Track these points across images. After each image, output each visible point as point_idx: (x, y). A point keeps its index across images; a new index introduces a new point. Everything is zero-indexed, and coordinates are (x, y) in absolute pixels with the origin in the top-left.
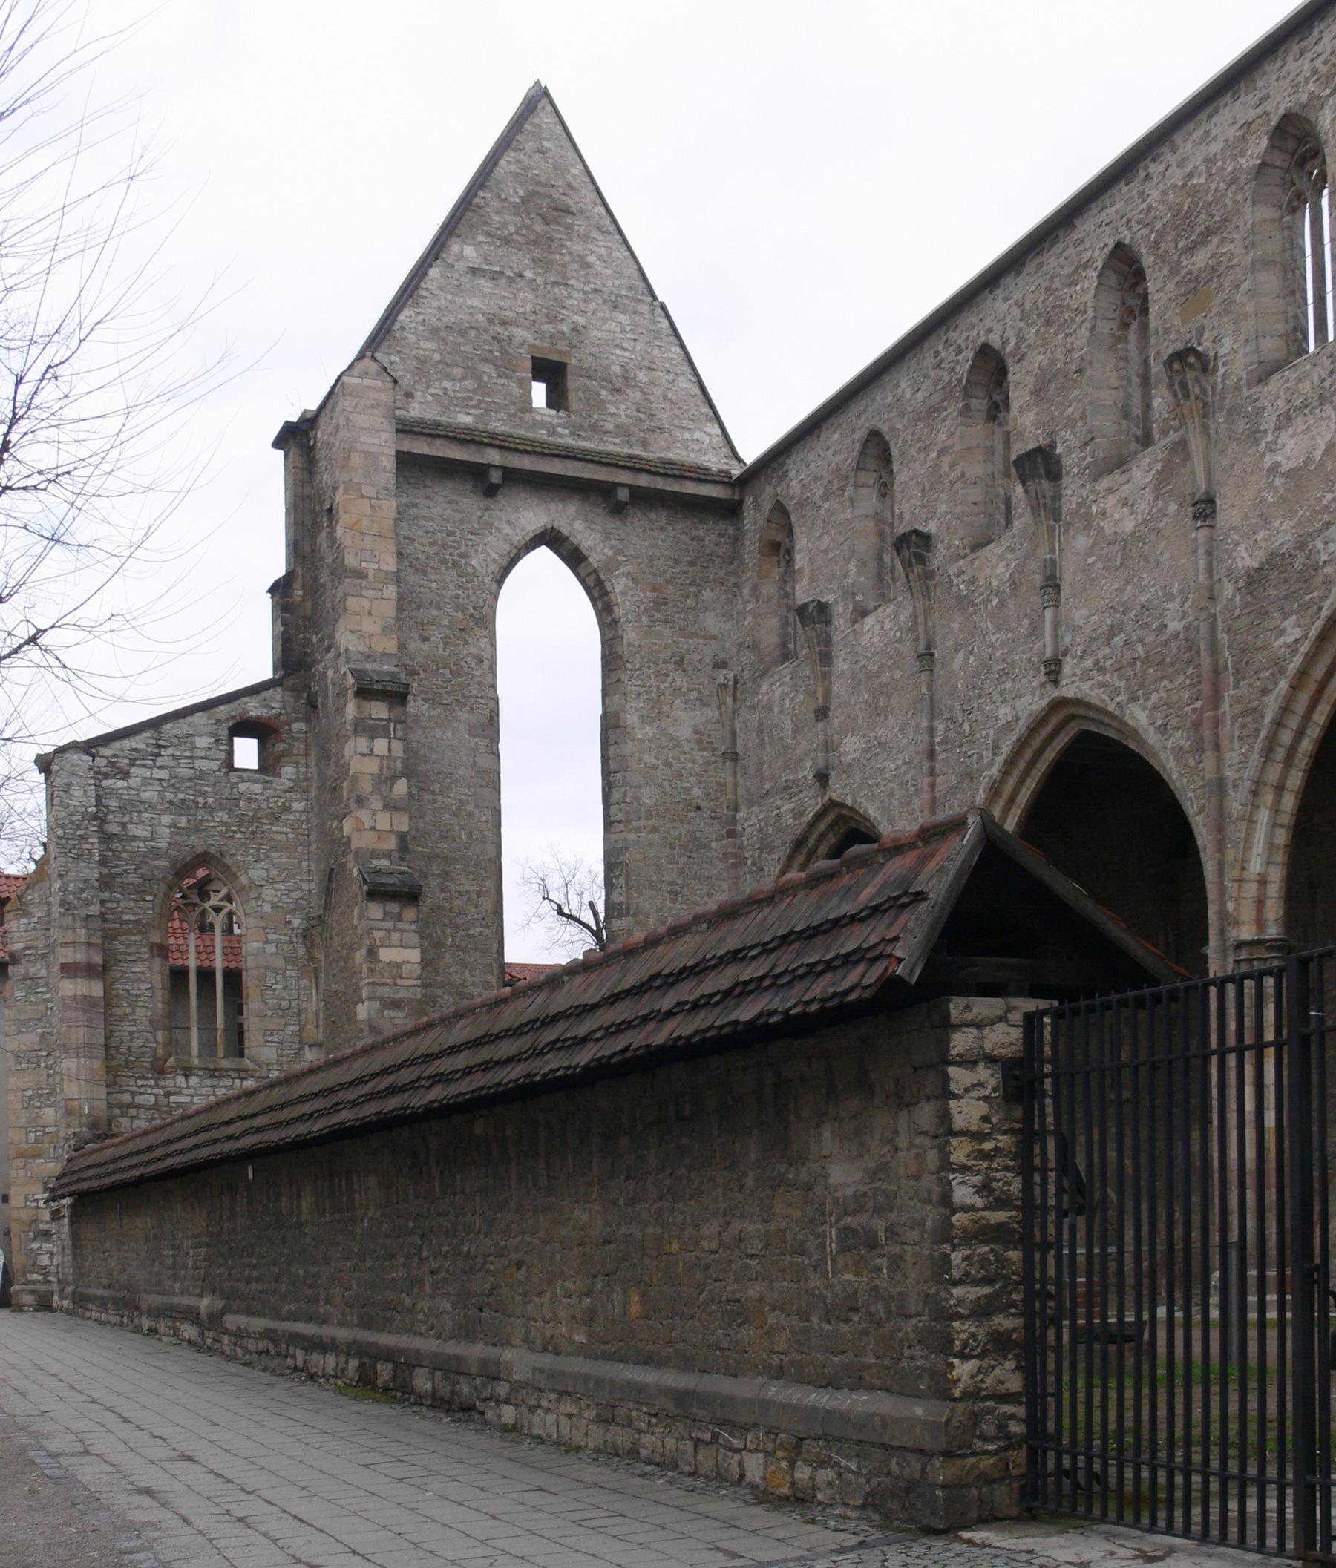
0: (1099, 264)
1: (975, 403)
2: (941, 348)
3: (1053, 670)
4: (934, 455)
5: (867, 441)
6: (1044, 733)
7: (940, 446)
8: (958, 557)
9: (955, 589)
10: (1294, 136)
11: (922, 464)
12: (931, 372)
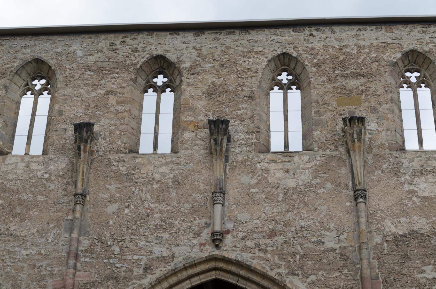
0: (270, 57)
1: (139, 79)
2: (118, 42)
3: (217, 239)
4: (103, 92)
5: (30, 62)
6: (191, 272)
7: (109, 89)
8: (119, 151)
9: (113, 168)
10: (409, 60)
11: (88, 92)
12: (104, 50)
